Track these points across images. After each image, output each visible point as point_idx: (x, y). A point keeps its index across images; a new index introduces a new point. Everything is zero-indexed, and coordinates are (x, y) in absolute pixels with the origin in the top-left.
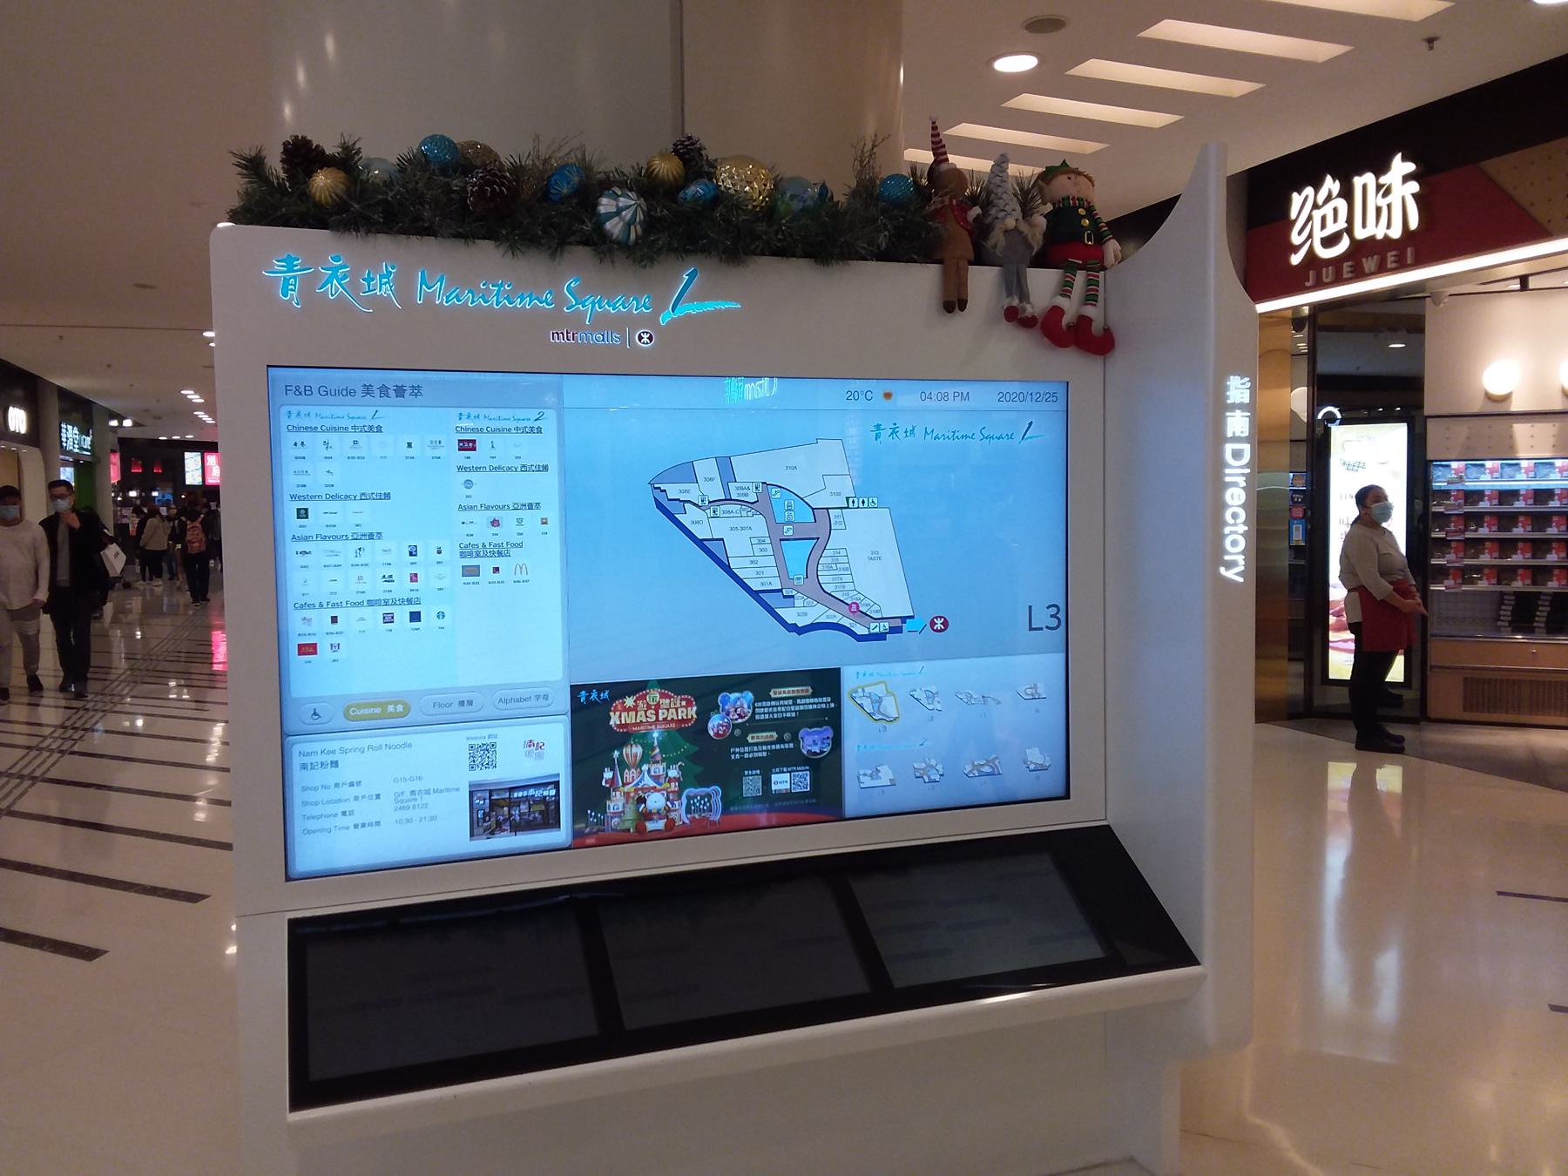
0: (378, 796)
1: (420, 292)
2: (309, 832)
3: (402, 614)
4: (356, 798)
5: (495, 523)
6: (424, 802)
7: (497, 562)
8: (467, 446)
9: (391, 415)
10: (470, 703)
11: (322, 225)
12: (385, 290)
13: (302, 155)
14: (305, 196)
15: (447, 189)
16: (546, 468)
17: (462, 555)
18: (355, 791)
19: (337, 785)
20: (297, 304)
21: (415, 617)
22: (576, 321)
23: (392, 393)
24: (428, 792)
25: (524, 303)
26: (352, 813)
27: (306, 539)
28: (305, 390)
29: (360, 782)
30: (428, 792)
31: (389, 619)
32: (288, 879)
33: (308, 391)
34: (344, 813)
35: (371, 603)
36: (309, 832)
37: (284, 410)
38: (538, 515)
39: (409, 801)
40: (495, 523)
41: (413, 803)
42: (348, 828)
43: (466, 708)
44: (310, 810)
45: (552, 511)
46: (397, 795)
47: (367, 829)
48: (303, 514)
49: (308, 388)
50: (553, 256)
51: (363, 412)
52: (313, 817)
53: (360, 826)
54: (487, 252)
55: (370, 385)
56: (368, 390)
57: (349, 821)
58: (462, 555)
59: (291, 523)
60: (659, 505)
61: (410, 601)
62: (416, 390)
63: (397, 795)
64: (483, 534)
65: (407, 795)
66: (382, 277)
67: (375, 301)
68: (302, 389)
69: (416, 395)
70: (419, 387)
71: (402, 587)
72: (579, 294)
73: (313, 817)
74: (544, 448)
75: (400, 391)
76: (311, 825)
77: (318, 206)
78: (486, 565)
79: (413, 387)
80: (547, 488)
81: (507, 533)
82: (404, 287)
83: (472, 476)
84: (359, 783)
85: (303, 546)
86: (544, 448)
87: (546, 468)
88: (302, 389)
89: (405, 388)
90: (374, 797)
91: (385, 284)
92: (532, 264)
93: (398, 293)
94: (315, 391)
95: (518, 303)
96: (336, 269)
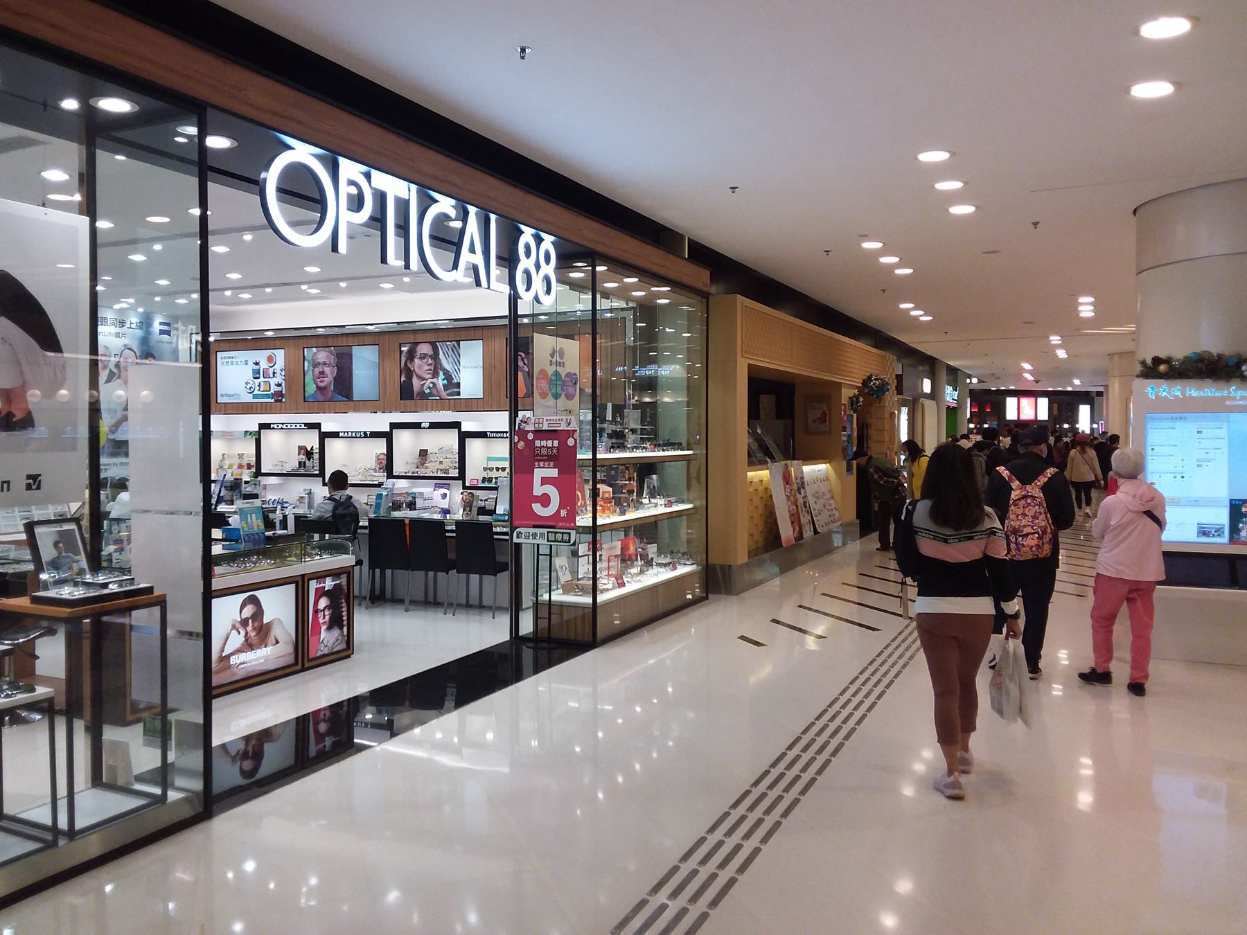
1: (1188, 393)
3: (1179, 476)
5: (1207, 453)
7: (1208, 463)
8: (1199, 432)
9: (1178, 425)
11: (1161, 378)
12: (1178, 393)
13: (1157, 361)
14: (1157, 371)
15: (1197, 367)
16: (1224, 438)
17: (1197, 461)
21: (1183, 477)
22: (1234, 399)
25: (1218, 394)
27: (1153, 456)
31: (1175, 477)
33: (1156, 419)
35: (1170, 473)
37: (1149, 424)
38: (1220, 451)
40: (1207, 453)
45: (1226, 450)
48: (1153, 449)
50: (1227, 382)
51: (1171, 424)
54: (1208, 381)
56: (1172, 419)
58: (1197, 461)
59: (1149, 451)
61: (1182, 473)
62: (1185, 418)
64: (1203, 455)
67: (1174, 396)
71: (1179, 469)
72: (1235, 391)
74: (1223, 432)
75: (1181, 418)
77: (1161, 373)
78: (1204, 464)
80: (1224, 445)
81: (1211, 456)
82: (1183, 393)
83: (1201, 440)
85: (1153, 458)
86: (1223, 432)
87: (1224, 438)
92: (1222, 384)
93: (1182, 394)
95: (1216, 394)
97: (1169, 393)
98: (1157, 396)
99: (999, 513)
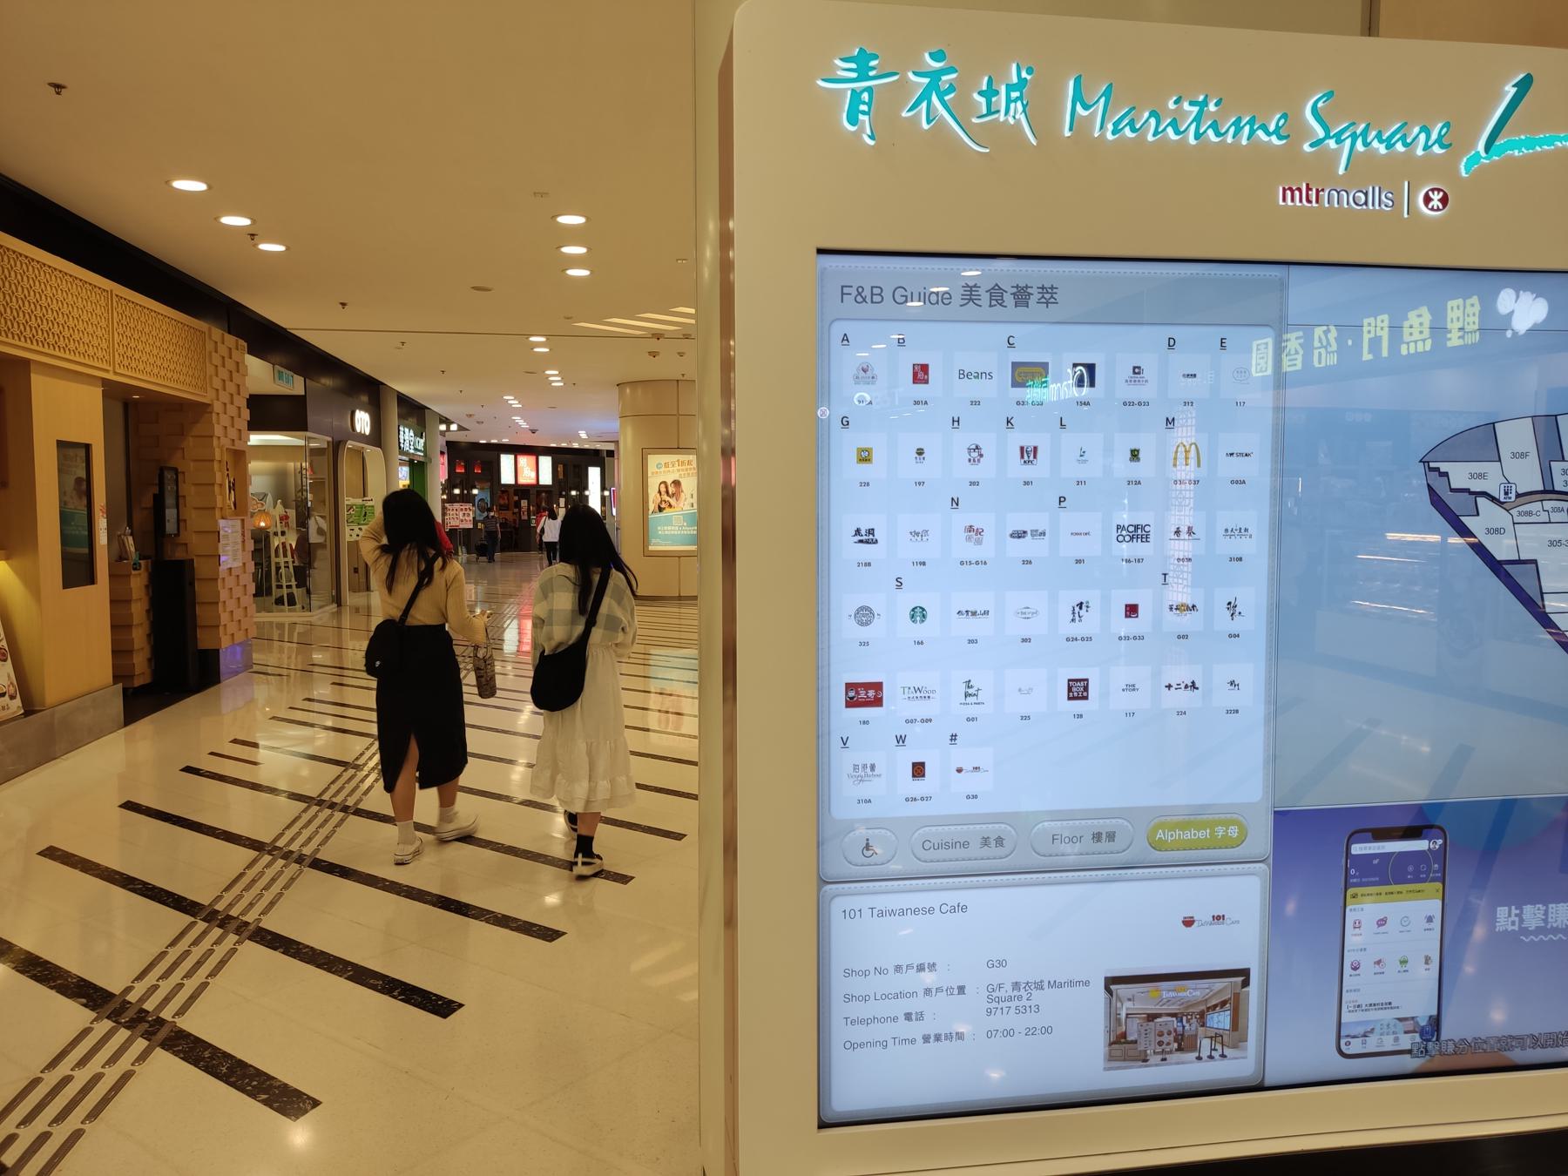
0: (961, 990)
2: (853, 1046)
4: (928, 991)
6: (1032, 1003)
10: (1111, 836)
18: (928, 978)
19: (898, 968)
20: (872, 137)
23: (1009, 300)
24: (1039, 986)
26: (920, 1016)
28: (872, 294)
29: (934, 965)
30: (1039, 986)
32: (823, 1125)
33: (876, 295)
34: (908, 1016)
36: (853, 1046)
39: (1010, 999)
41: (1017, 1003)
42: (913, 1041)
43: (1104, 845)
44: (858, 1010)
46: (991, 989)
47: (945, 1043)
49: (876, 291)
52: (861, 1022)
53: (932, 1040)
55: (975, 286)
57: (916, 1030)
60: (1437, 501)
62: (1048, 294)
63: (991, 989)
65: (1008, 990)
66: (1010, 88)
68: (867, 293)
69: (1047, 303)
70: (1052, 288)
73: (861, 1022)
76: (860, 1034)
79: (1043, 288)
82: (1042, 109)
84: (932, 966)
88: (867, 293)
89: (1029, 290)
90: (956, 992)
91: (1015, 101)
94: (887, 294)
96: (935, 75)
97: (960, 111)
98: (886, 121)
99: (59, 853)
